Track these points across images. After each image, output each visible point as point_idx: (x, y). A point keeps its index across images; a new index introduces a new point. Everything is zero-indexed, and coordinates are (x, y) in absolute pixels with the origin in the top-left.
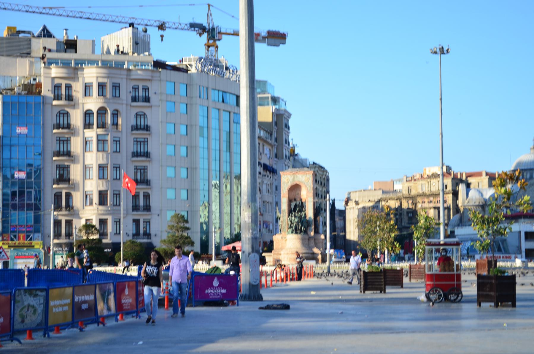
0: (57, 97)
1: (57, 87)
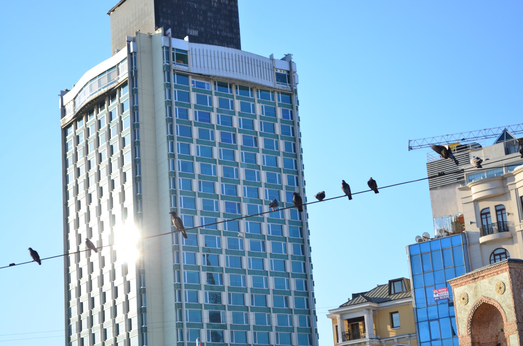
0: (485, 231)
1: (484, 214)
